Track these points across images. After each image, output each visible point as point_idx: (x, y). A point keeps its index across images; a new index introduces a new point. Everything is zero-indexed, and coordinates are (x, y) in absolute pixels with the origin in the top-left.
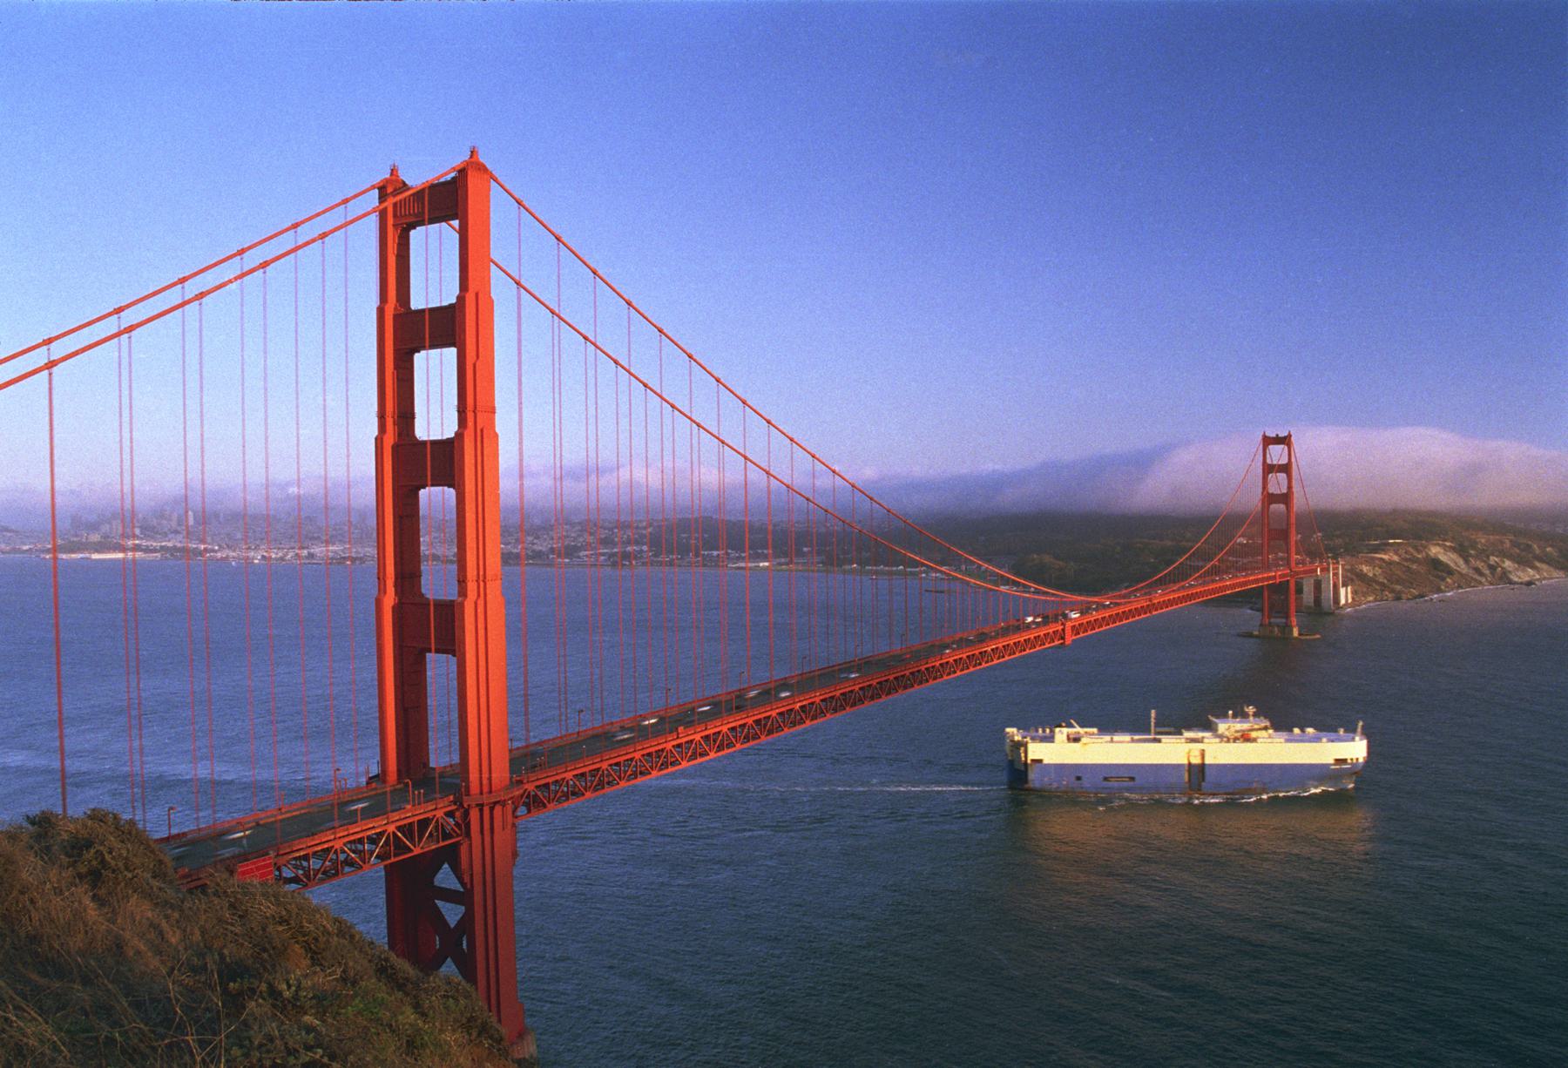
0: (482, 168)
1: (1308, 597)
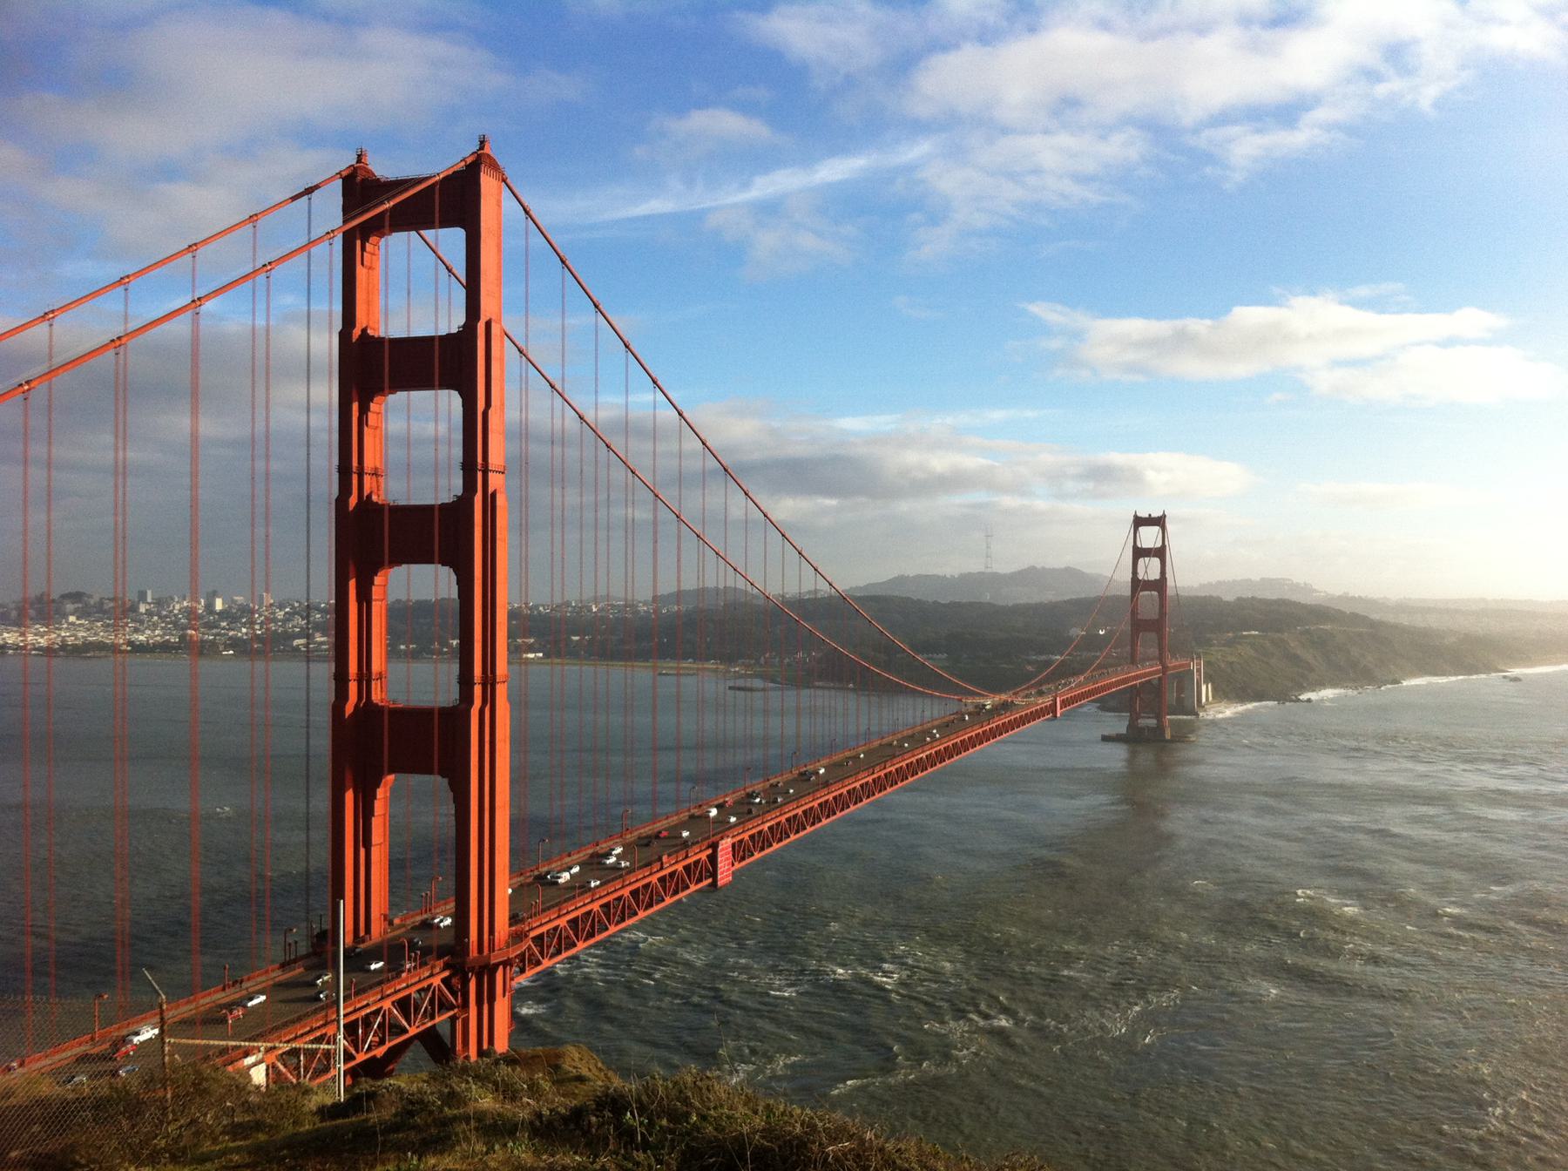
0: (494, 166)
1: (1171, 696)
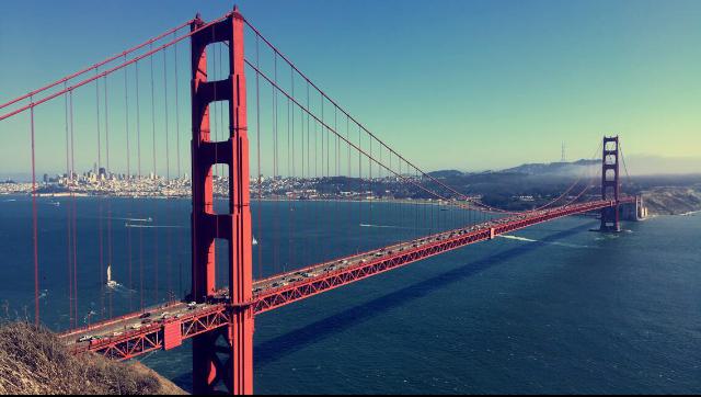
0: (240, 18)
